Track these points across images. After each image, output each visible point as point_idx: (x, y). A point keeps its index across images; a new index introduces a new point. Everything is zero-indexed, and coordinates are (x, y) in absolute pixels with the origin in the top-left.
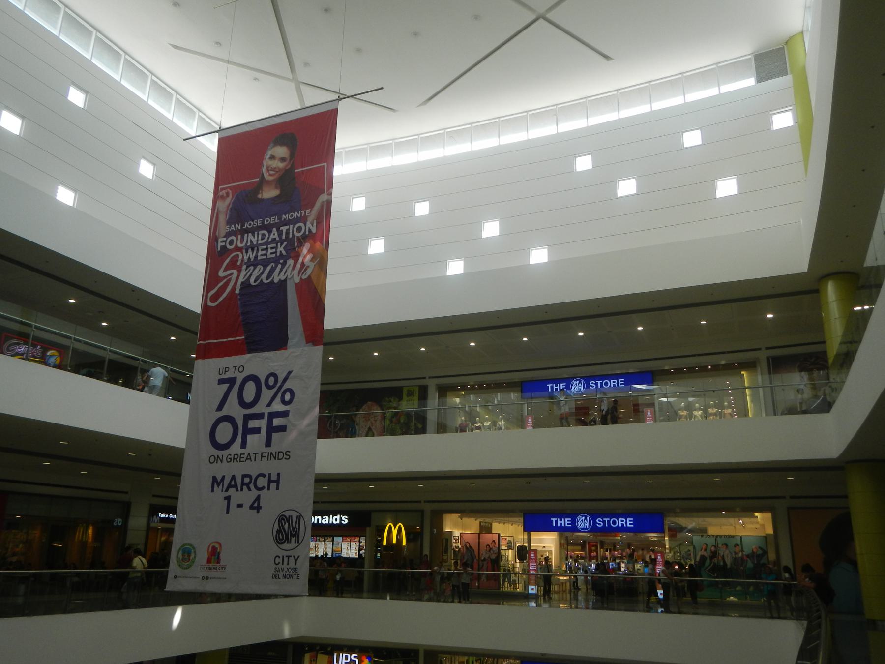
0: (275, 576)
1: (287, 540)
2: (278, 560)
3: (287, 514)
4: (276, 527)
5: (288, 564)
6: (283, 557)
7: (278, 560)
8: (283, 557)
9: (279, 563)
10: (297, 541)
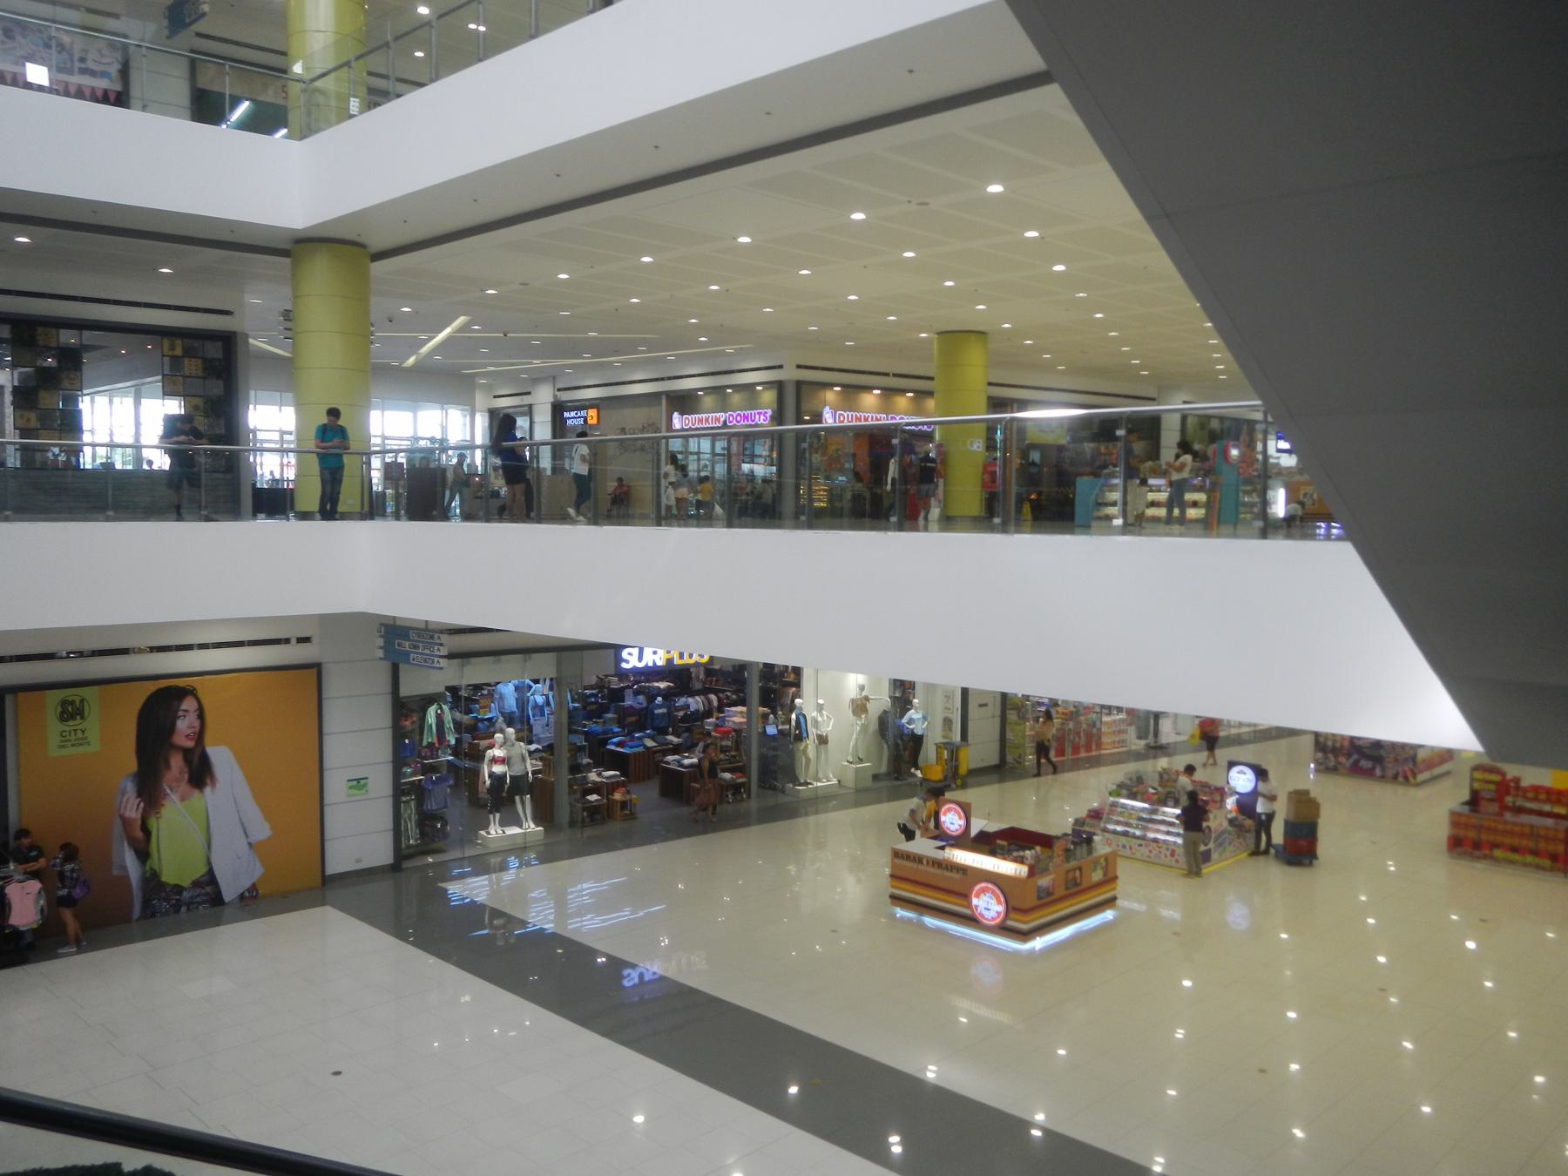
1: (72, 717)
3: (70, 699)
4: (59, 709)
5: (76, 735)
6: (70, 731)
7: (64, 734)
10: (82, 718)
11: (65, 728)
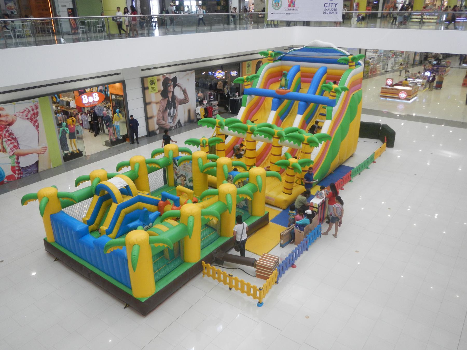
0: (325, 13)
2: (326, 5)
6: (329, 3)
7: (326, 5)
8: (329, 3)
9: (327, 6)
11: (152, 87)
